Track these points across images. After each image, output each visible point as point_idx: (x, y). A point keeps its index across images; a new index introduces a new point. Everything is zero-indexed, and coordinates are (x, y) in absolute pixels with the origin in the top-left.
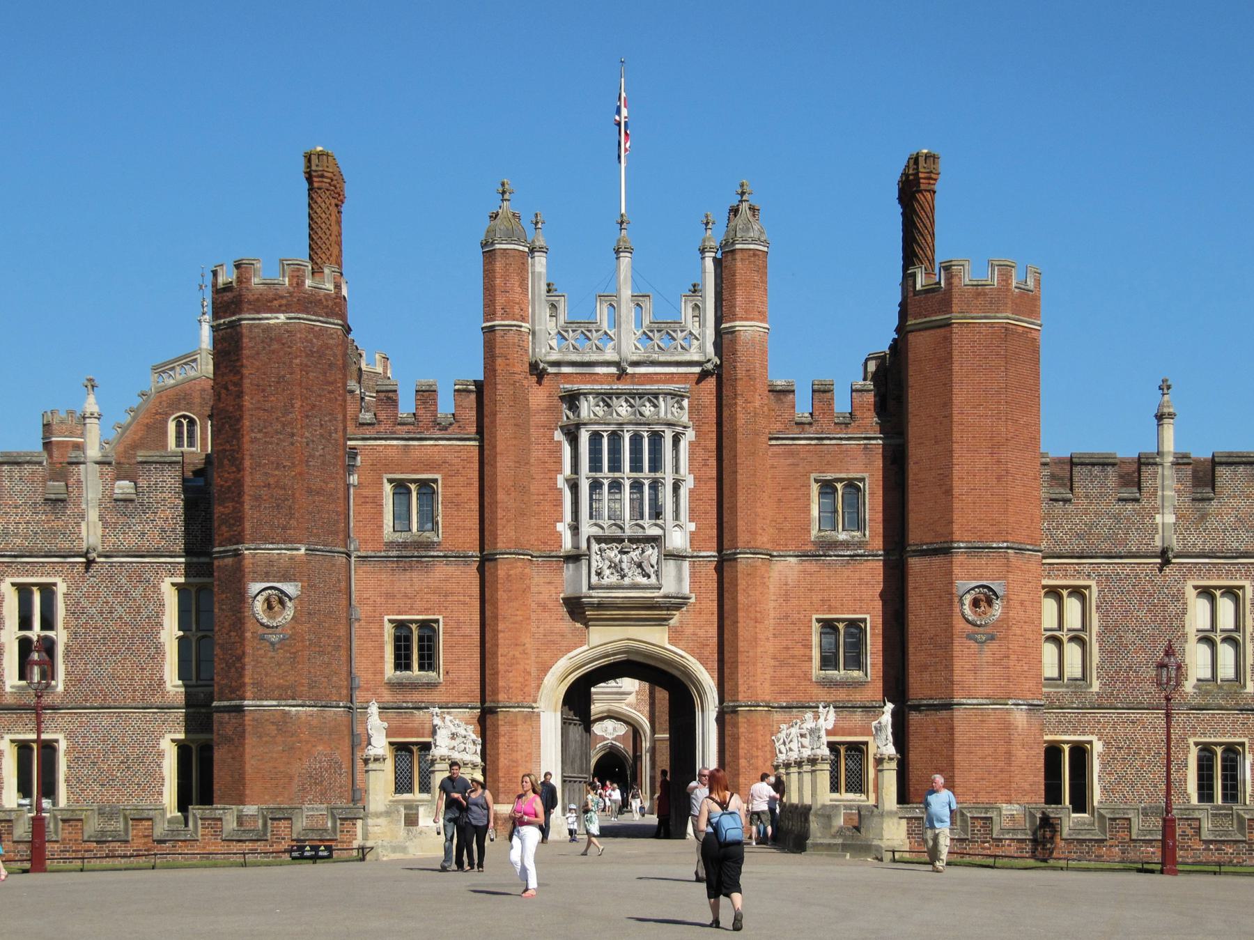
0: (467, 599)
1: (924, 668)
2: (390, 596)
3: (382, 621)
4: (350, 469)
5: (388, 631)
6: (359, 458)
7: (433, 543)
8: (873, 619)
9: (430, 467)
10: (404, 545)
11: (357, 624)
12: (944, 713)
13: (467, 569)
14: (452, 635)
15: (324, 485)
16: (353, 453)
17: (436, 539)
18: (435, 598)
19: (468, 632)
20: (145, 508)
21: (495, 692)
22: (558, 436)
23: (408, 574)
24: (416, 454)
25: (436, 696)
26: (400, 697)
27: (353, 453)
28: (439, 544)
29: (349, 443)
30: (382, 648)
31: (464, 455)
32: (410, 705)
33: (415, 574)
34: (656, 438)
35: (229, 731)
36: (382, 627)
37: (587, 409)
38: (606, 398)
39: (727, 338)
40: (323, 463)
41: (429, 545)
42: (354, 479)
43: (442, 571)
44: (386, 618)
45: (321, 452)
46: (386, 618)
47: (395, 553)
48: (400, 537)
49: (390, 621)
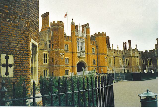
1: (102, 63)
8: (96, 60)
10: (66, 51)
12: (104, 67)
20: (41, 45)
21: (74, 65)
22: (77, 42)
25: (69, 65)
34: (84, 43)
35: (57, 68)
37: (80, 40)
38: (81, 39)
39: (88, 35)
41: (68, 51)
43: (69, 53)
48: (66, 50)
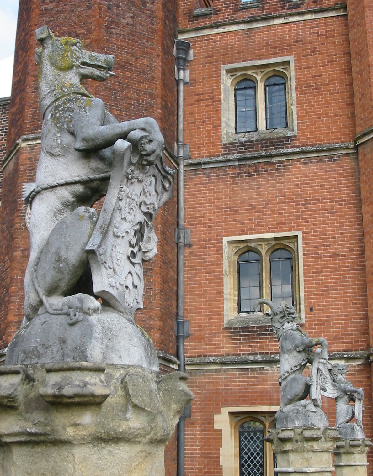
0: (336, 206)
2: (230, 210)
3: (220, 243)
4: (183, 62)
5: (229, 255)
6: (191, 52)
7: (286, 138)
9: (280, 48)
10: (250, 145)
11: (187, 251)
13: (334, 166)
14: (316, 256)
15: (132, 60)
16: (185, 47)
17: (289, 134)
18: (293, 207)
19: (339, 250)
23: (254, 180)
24: (261, 38)
26: (245, 347)
27: (185, 47)
28: (294, 138)
29: (180, 37)
30: (220, 280)
31: (321, 30)
32: (259, 358)
33: (263, 180)
36: (220, 251)
40: (131, 33)
42: (185, 75)
44: (225, 240)
45: (130, 20)
46: (225, 240)
47: (236, 156)
49: (230, 242)
